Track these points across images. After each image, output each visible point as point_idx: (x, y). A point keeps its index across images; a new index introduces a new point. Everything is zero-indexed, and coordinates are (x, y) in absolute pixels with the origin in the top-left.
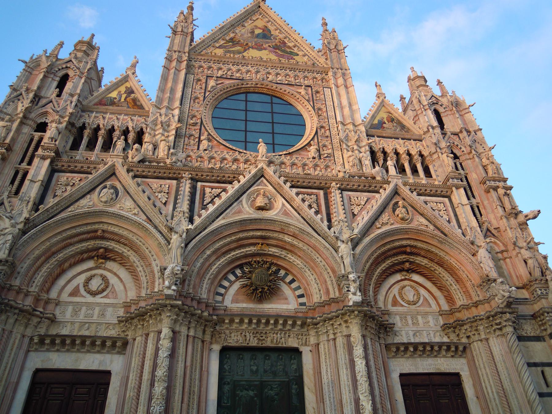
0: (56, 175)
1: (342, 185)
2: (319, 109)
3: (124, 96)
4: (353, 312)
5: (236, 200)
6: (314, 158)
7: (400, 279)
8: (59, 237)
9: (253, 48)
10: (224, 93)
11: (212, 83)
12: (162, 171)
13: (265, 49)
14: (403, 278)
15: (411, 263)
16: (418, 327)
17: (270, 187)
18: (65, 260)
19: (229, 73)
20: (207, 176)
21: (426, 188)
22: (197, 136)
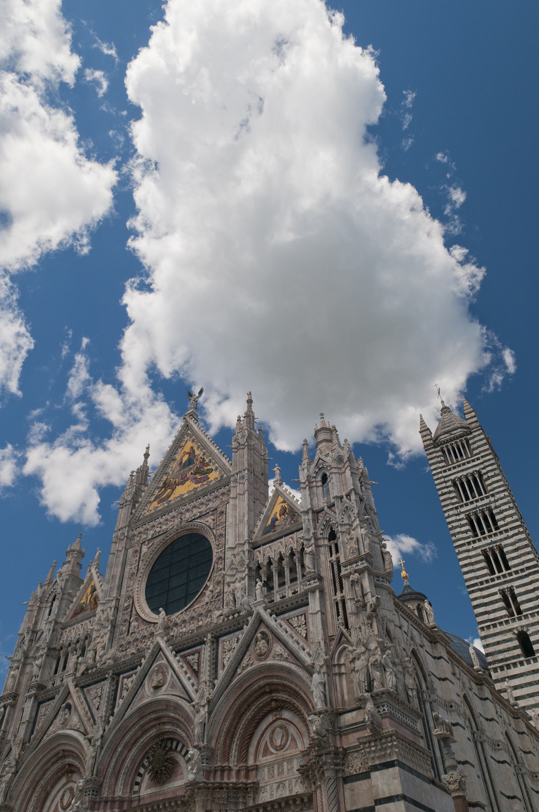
0: (41, 706)
1: (217, 632)
2: (221, 535)
3: (89, 597)
4: (194, 789)
5: (140, 686)
6: (207, 603)
7: (271, 721)
8: (38, 767)
9: (178, 485)
10: (154, 554)
11: (145, 549)
12: (96, 676)
13: (188, 480)
14: (274, 718)
15: (276, 700)
16: (283, 776)
17: (164, 661)
18: (47, 783)
20: (124, 667)
21: (286, 604)
22: (129, 619)
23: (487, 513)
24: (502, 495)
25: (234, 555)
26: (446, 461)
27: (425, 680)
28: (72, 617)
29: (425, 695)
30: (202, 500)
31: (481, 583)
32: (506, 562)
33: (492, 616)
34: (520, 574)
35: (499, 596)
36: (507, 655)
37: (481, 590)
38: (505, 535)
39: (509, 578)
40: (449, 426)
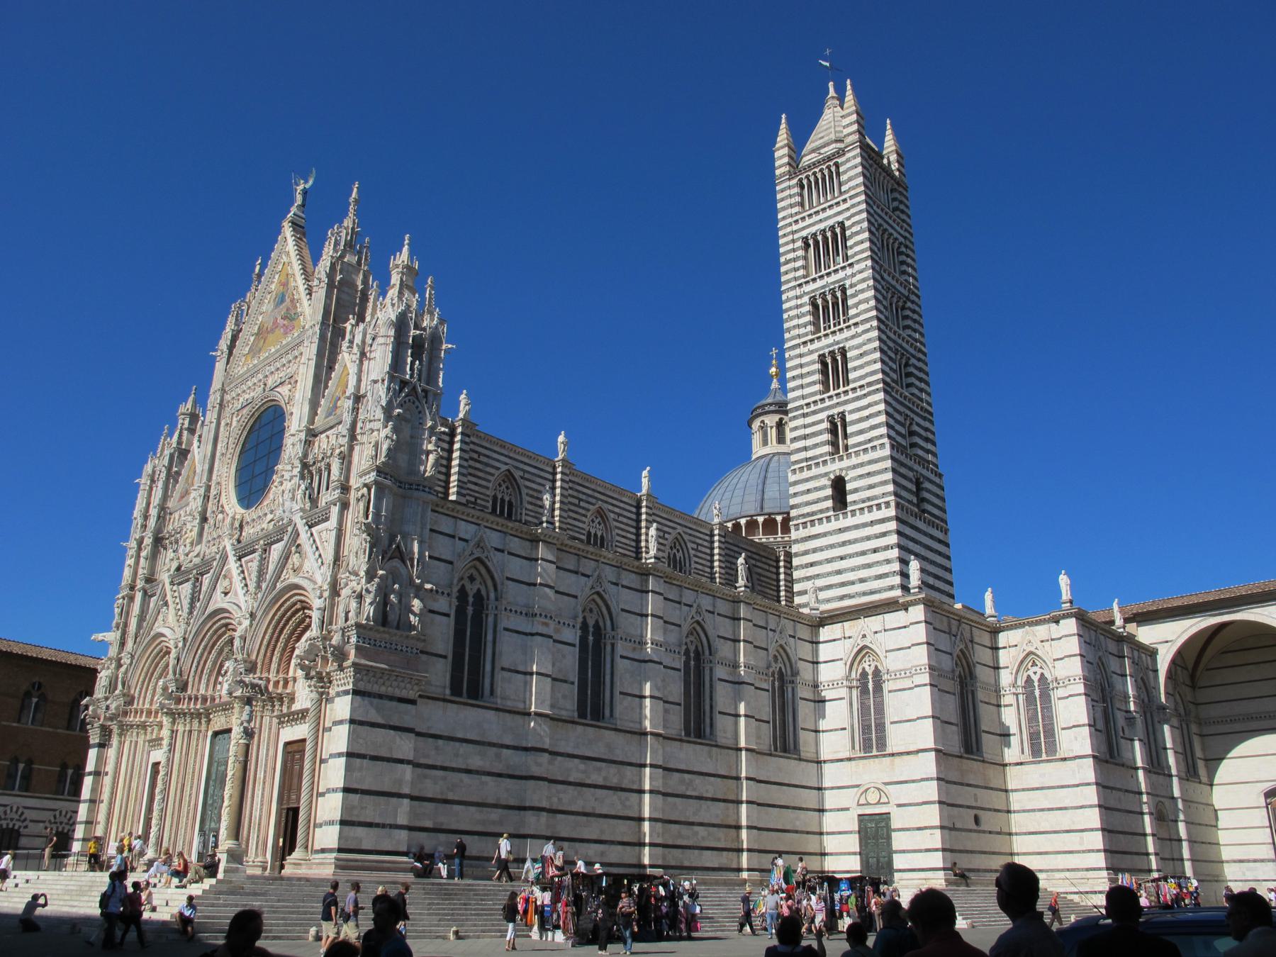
11: (235, 419)
19: (247, 396)
23: (839, 294)
24: (862, 265)
25: (293, 445)
26: (802, 204)
27: (496, 589)
28: (179, 500)
29: (490, 607)
30: (284, 361)
31: (808, 405)
32: (846, 371)
33: (810, 454)
34: (859, 393)
35: (826, 425)
36: (815, 508)
37: (804, 415)
38: (853, 331)
39: (843, 398)
40: (822, 137)
